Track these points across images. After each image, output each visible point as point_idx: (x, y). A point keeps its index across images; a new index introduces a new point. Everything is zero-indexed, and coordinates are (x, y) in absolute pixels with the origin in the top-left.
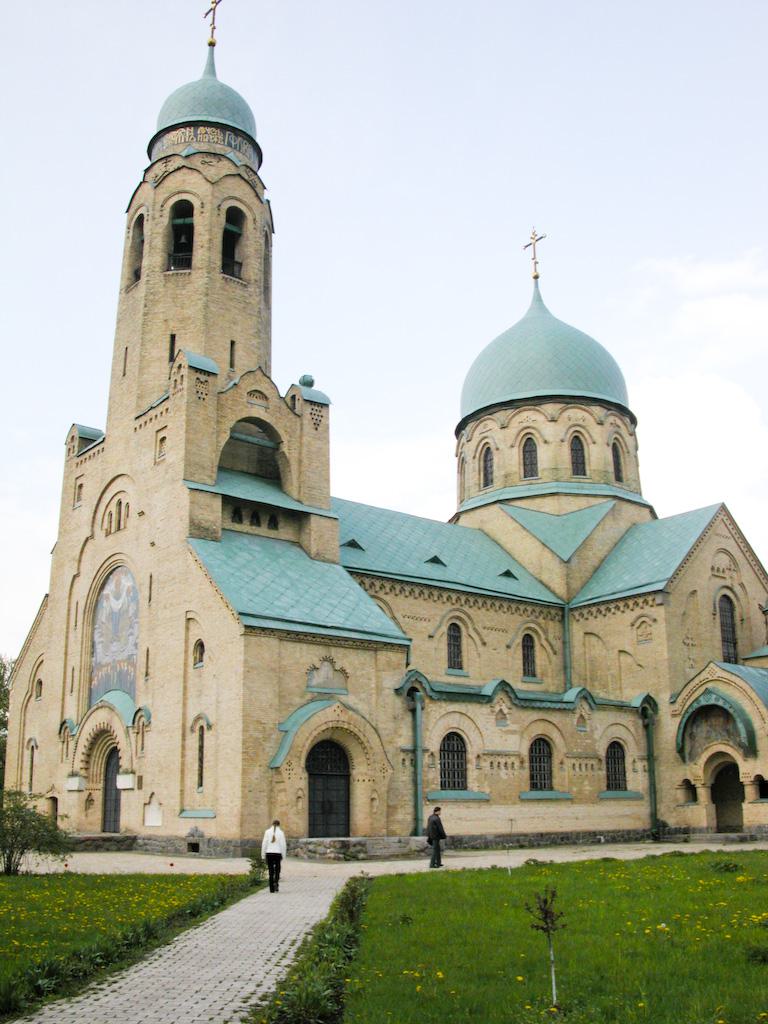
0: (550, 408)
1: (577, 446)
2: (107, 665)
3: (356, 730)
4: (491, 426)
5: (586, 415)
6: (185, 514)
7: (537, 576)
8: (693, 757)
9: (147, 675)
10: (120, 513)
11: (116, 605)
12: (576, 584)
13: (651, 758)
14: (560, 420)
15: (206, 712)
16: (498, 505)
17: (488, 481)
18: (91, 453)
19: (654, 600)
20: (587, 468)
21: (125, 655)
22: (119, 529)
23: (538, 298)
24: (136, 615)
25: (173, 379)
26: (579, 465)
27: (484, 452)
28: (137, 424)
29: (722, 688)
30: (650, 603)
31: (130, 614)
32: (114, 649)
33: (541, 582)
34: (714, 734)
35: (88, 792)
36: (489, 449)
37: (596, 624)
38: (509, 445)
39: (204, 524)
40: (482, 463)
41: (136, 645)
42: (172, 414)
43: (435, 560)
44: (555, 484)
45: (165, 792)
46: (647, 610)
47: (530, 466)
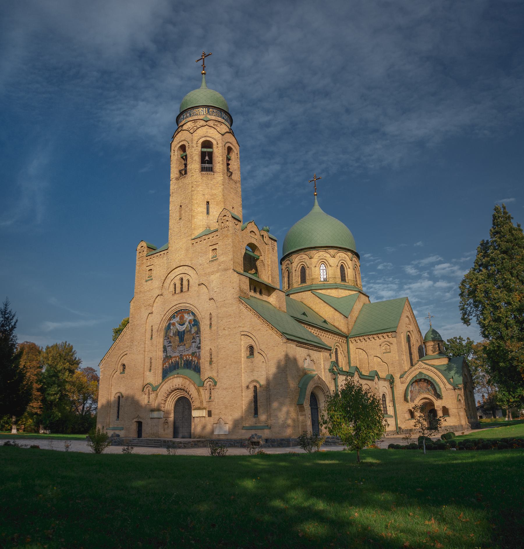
0: (332, 251)
2: (175, 357)
3: (322, 387)
5: (346, 256)
6: (236, 285)
7: (332, 323)
8: (412, 400)
9: (211, 362)
10: (182, 285)
11: (182, 328)
12: (350, 328)
13: (393, 401)
15: (258, 379)
16: (310, 292)
17: (303, 280)
18: (157, 254)
20: (347, 278)
21: (190, 352)
22: (182, 291)
24: (198, 332)
25: (220, 222)
26: (343, 278)
27: (300, 268)
28: (193, 242)
29: (425, 372)
31: (192, 333)
32: (181, 349)
33: (334, 326)
34: (422, 390)
37: (363, 344)
38: (314, 265)
39: (245, 291)
40: (299, 273)
41: (199, 348)
42: (221, 238)
43: (304, 314)
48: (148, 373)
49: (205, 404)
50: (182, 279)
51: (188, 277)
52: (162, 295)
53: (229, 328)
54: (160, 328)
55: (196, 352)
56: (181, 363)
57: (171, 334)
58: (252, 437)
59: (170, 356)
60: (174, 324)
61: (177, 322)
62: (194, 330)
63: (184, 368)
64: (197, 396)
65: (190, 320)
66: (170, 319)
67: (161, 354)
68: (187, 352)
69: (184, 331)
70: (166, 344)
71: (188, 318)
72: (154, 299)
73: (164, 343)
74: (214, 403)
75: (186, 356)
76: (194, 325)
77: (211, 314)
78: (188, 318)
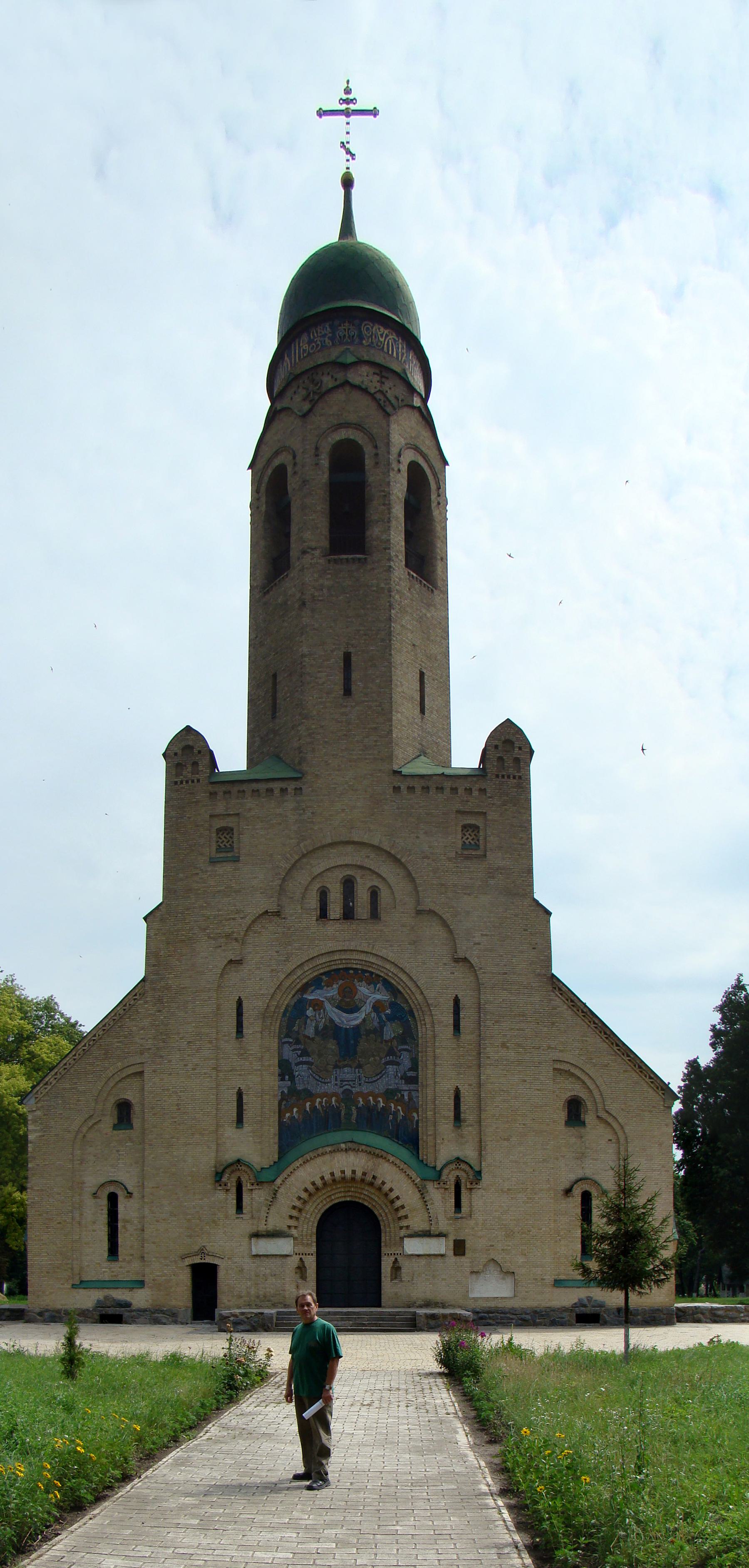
2: (325, 1095)
21: (381, 1086)
22: (348, 914)
24: (409, 1036)
32: (348, 1077)
35: (297, 1258)
45: (521, 1260)
48: (230, 1131)
49: (443, 1225)
50: (349, 885)
51: (376, 882)
52: (278, 914)
53: (519, 1045)
54: (272, 1009)
55: (398, 1090)
56: (349, 1114)
57: (310, 1031)
58: (581, 1304)
59: (306, 1090)
60: (317, 1005)
61: (331, 1000)
62: (391, 1031)
63: (358, 1128)
64: (419, 1204)
65: (378, 1002)
66: (304, 989)
67: (272, 1082)
68: (372, 1086)
69: (357, 1028)
70: (289, 1053)
71: (370, 995)
72: (248, 921)
73: (280, 1054)
74: (472, 1223)
75: (365, 1096)
76: (390, 1018)
77: (457, 1001)
78: (370, 995)
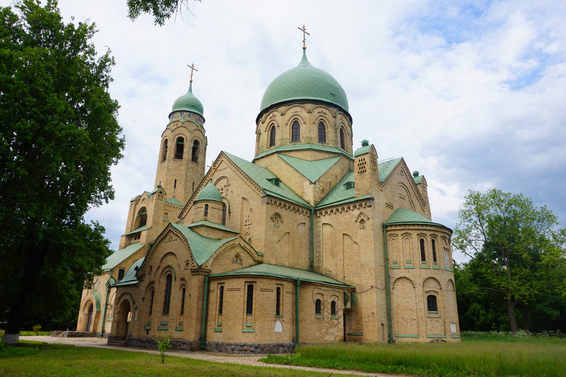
0: (309, 106)
1: (322, 127)
4: (277, 114)
14: (313, 113)
16: (276, 155)
17: (272, 143)
19: (366, 204)
23: (305, 57)
26: (322, 138)
30: (364, 206)
36: (274, 127)
44: (309, 145)
46: (362, 210)
47: (295, 137)
